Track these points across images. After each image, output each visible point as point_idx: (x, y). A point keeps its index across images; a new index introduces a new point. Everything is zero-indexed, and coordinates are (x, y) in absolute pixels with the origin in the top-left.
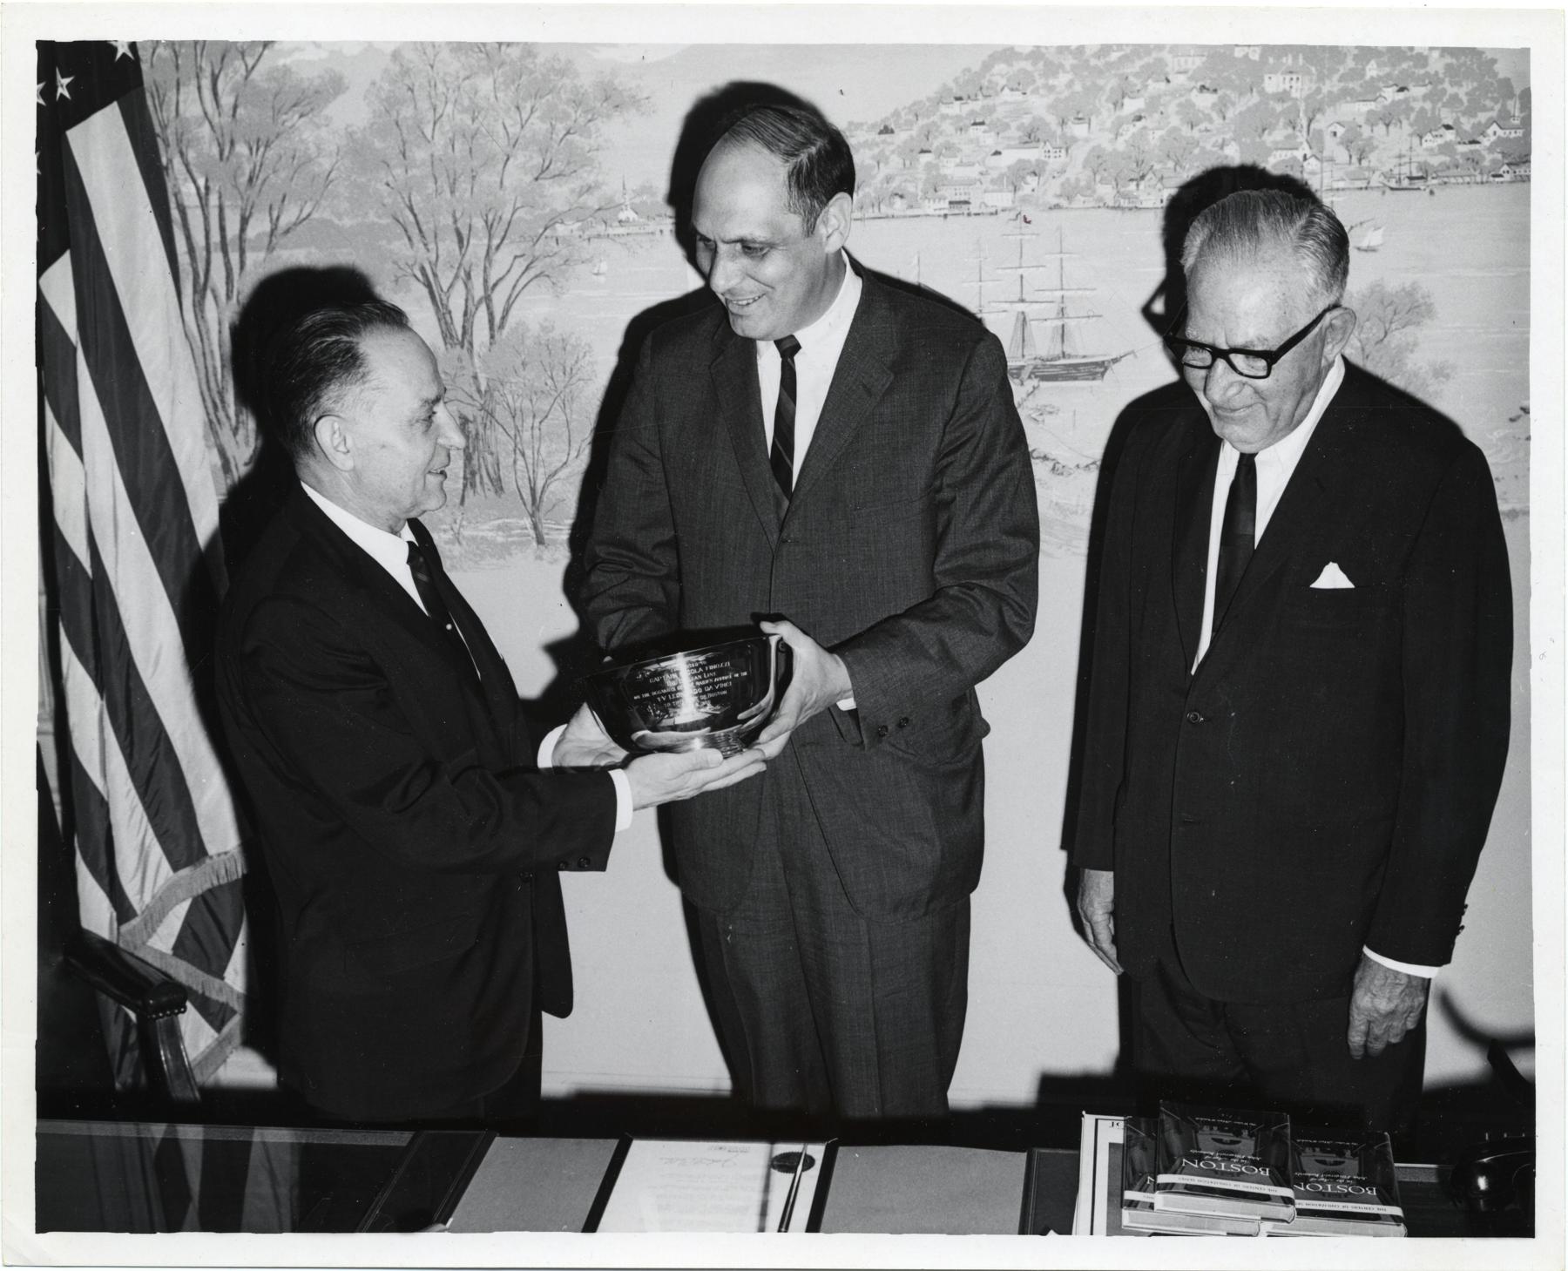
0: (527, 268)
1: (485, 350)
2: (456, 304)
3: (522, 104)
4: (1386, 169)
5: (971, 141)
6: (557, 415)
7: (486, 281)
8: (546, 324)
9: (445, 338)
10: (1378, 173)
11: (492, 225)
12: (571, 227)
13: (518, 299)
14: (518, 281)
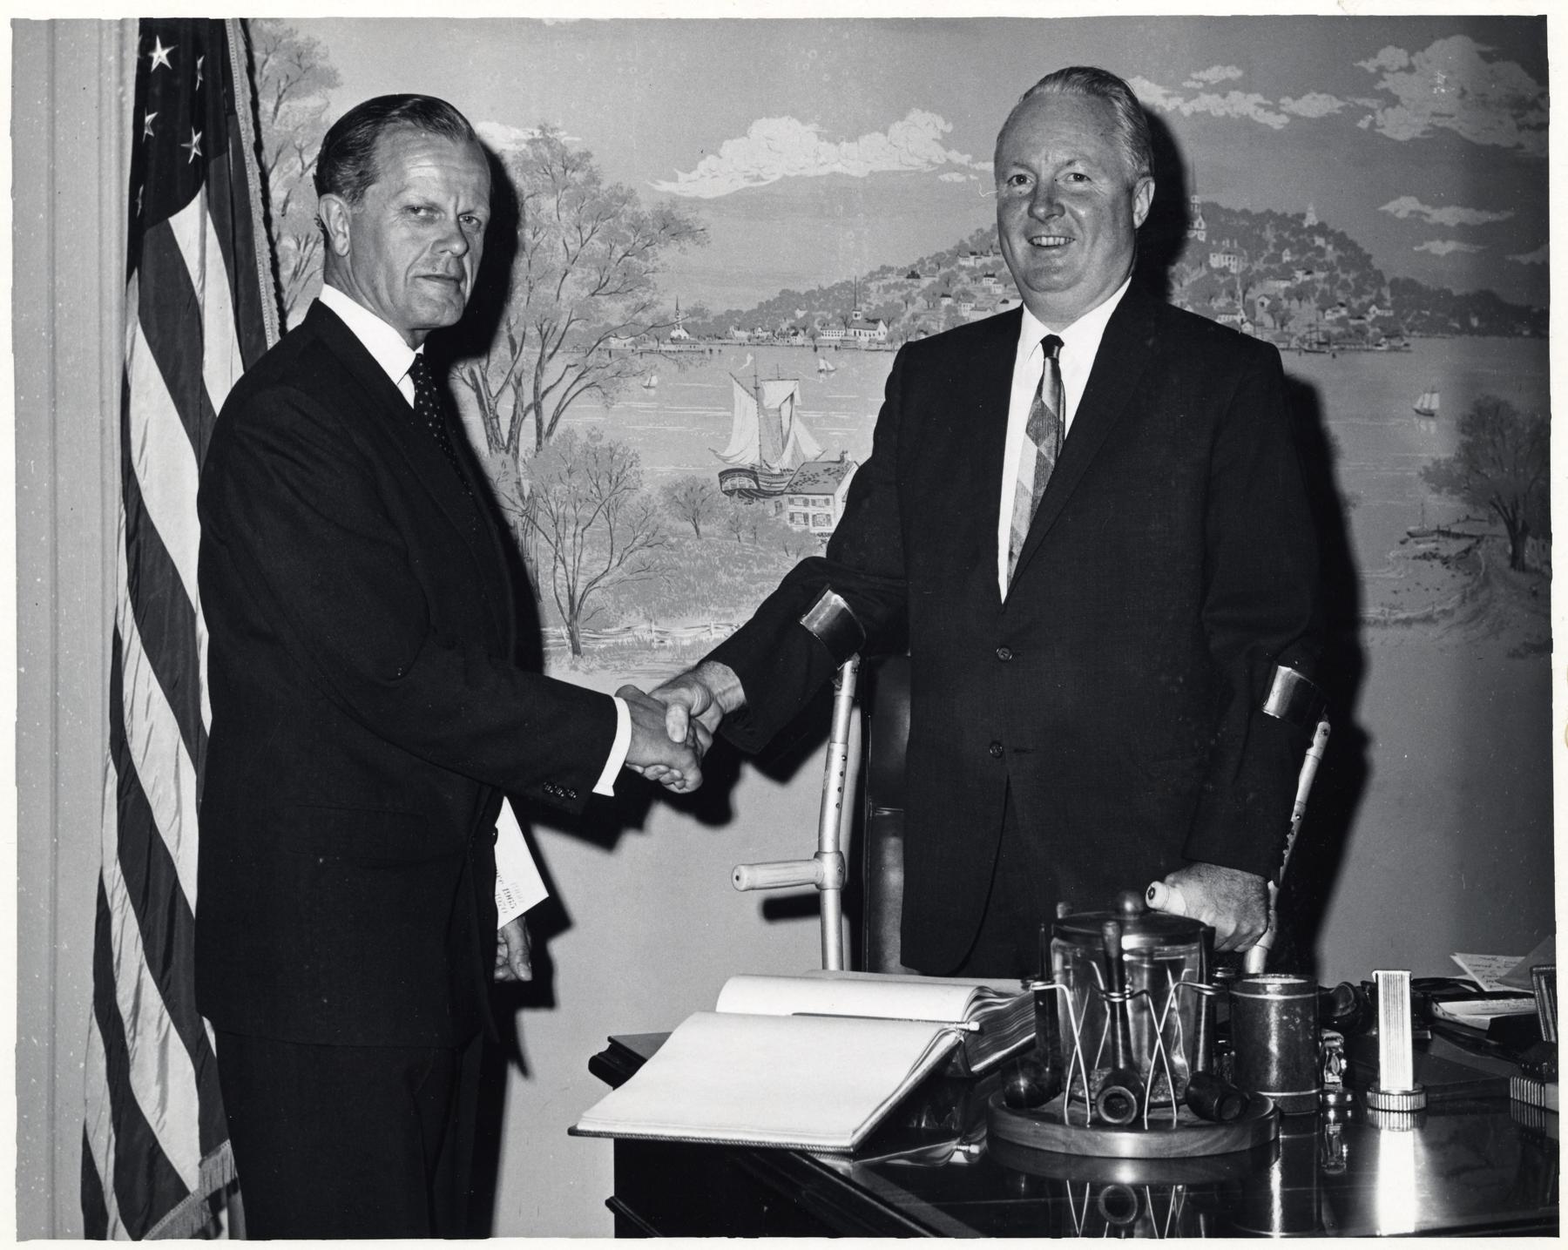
0: (578, 378)
1: (530, 456)
2: (505, 409)
3: (583, 225)
4: (1300, 335)
5: (984, 290)
6: (601, 524)
7: (536, 388)
8: (594, 433)
9: (489, 445)
10: (1295, 338)
11: (546, 334)
12: (624, 342)
13: (569, 406)
14: (569, 389)
